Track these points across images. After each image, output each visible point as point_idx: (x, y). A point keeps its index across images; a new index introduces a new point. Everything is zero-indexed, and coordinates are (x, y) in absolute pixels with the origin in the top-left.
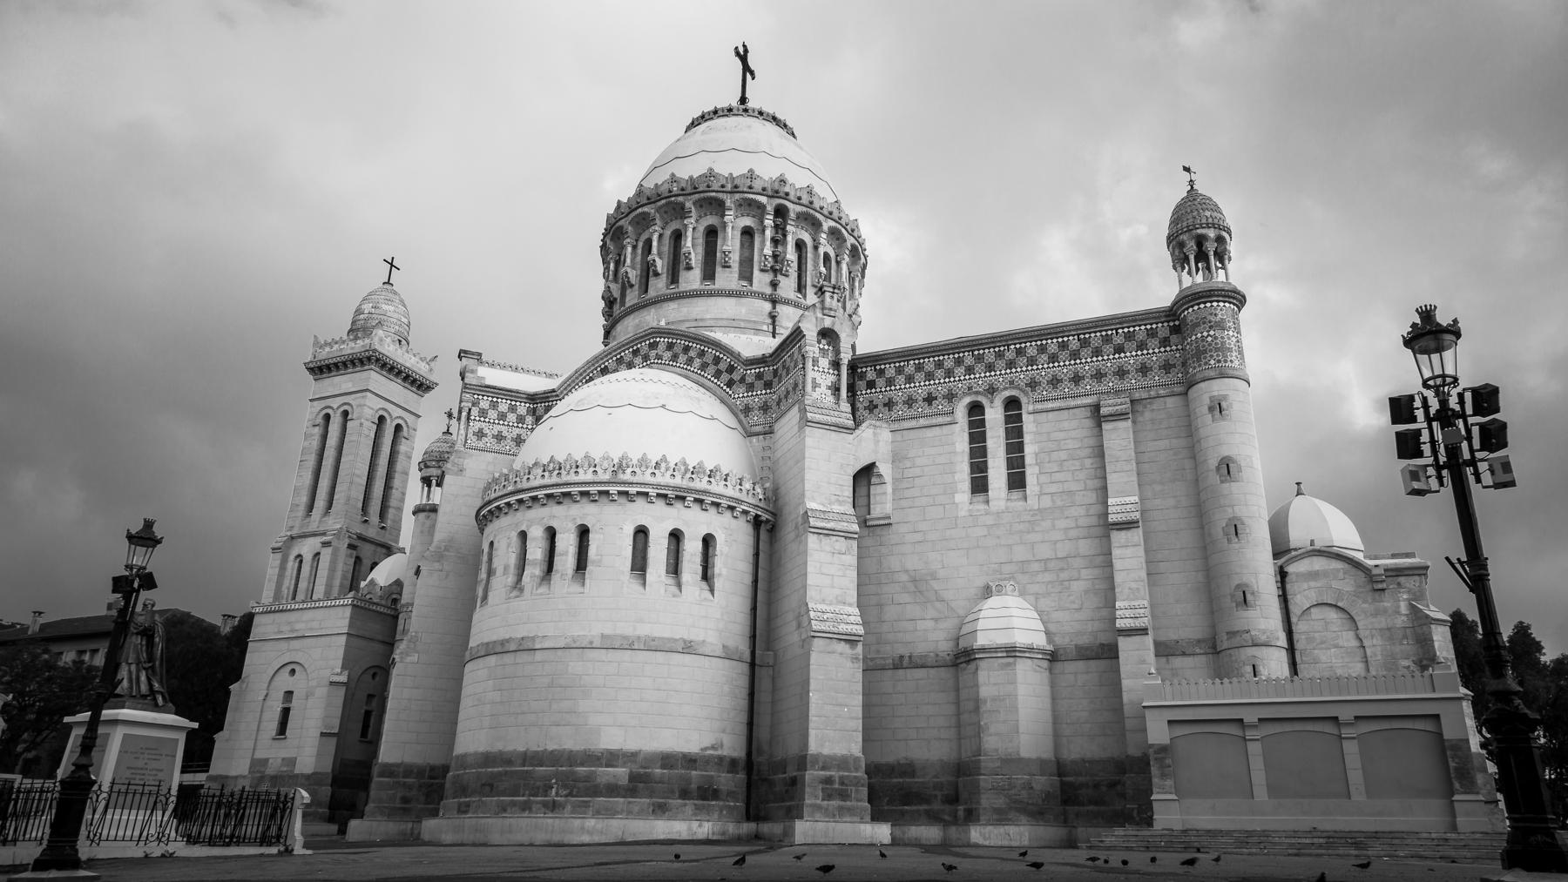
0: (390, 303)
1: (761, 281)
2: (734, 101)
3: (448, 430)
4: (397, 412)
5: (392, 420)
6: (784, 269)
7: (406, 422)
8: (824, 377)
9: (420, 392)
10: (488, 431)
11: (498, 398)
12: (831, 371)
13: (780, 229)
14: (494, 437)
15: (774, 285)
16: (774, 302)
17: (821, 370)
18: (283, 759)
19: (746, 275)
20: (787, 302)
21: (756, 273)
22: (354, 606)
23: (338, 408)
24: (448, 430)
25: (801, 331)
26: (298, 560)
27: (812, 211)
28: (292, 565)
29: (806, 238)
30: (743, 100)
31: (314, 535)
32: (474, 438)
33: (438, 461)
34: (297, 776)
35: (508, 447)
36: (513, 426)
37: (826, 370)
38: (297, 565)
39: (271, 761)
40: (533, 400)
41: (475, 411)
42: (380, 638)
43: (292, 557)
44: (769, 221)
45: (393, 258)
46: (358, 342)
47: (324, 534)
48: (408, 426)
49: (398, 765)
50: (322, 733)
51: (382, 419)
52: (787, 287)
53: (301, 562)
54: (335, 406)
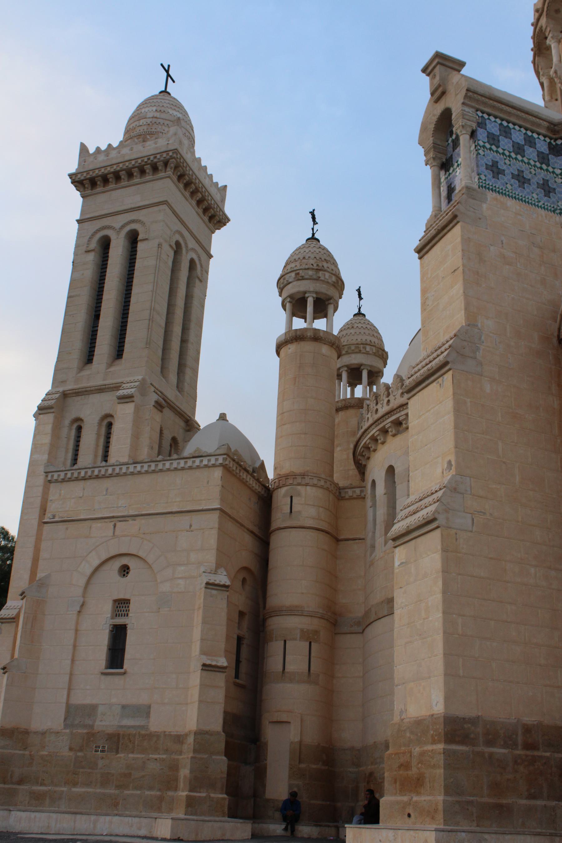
0: (177, 109)
3: (313, 234)
4: (192, 243)
5: (187, 251)
7: (199, 257)
9: (211, 225)
10: (504, 167)
11: (508, 122)
14: (513, 176)
18: (124, 707)
22: (225, 467)
23: (123, 227)
24: (313, 234)
26: (75, 426)
28: (70, 434)
31: (101, 390)
32: (490, 175)
33: (318, 270)
34: (156, 736)
35: (534, 195)
36: (535, 166)
38: (73, 433)
39: (101, 709)
40: (554, 132)
41: (482, 135)
42: (251, 527)
43: (67, 422)
45: (169, 66)
46: (148, 143)
47: (117, 387)
48: (201, 266)
49: (474, 721)
50: (204, 665)
51: (178, 244)
53: (79, 429)
54: (117, 226)
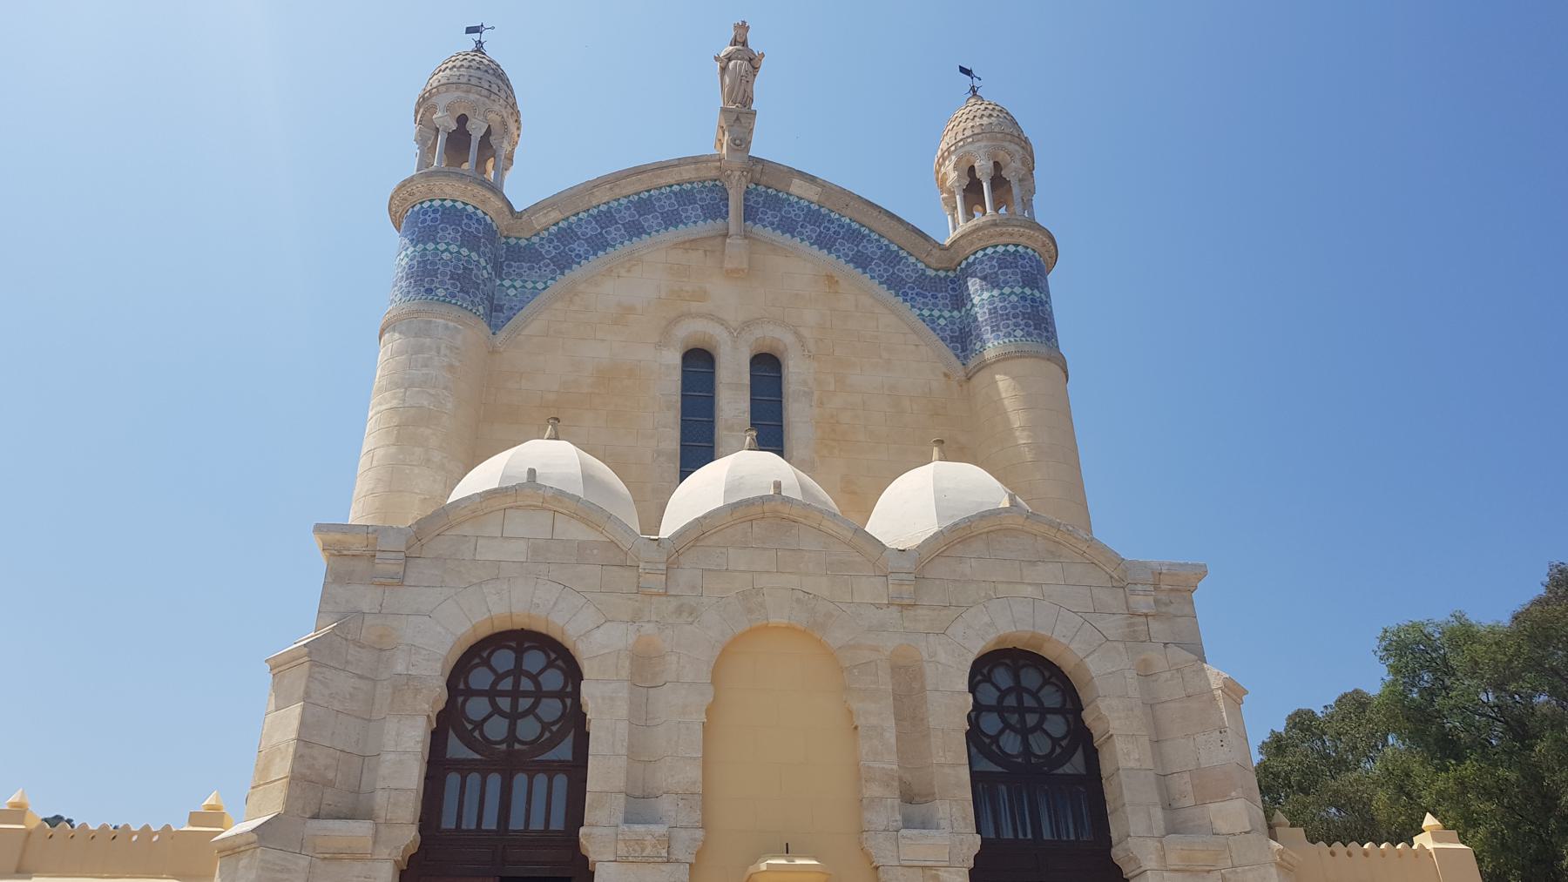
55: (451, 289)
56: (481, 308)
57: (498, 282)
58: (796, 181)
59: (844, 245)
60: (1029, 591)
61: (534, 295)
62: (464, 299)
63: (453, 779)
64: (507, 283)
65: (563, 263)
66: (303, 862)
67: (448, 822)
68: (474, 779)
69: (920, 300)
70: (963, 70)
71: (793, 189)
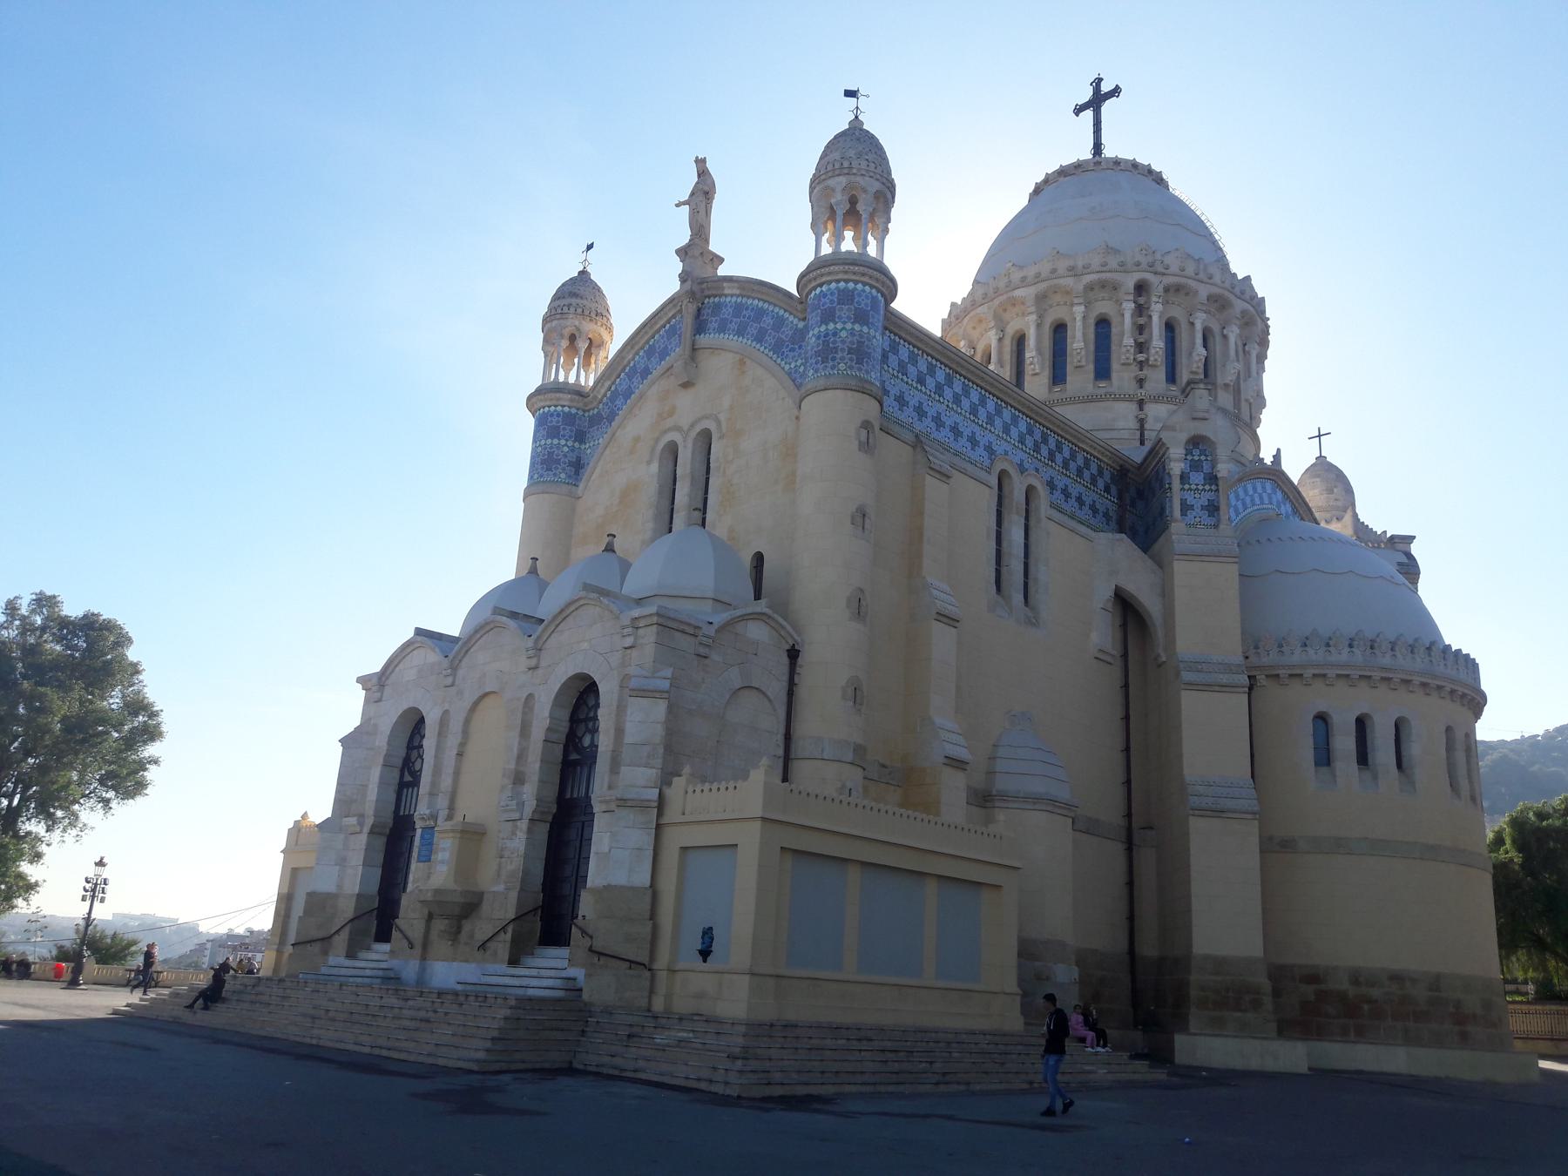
1: (1122, 377)
2: (1086, 154)
6: (1152, 358)
8: (1197, 496)
12: (1207, 487)
13: (1140, 310)
15: (1141, 382)
16: (1141, 403)
17: (1193, 487)
19: (1102, 371)
20: (1157, 399)
21: (1115, 366)
25: (1164, 444)
27: (1183, 280)
29: (1177, 313)
30: (1098, 147)
37: (1200, 487)
44: (1129, 307)
52: (1157, 378)
55: (541, 472)
56: (563, 476)
57: (583, 447)
58: (725, 284)
59: (755, 329)
60: (585, 645)
61: (597, 448)
62: (548, 475)
63: (405, 790)
64: (587, 446)
65: (611, 417)
66: (342, 836)
67: (402, 813)
68: (410, 790)
69: (791, 354)
70: (850, 94)
71: (727, 291)
